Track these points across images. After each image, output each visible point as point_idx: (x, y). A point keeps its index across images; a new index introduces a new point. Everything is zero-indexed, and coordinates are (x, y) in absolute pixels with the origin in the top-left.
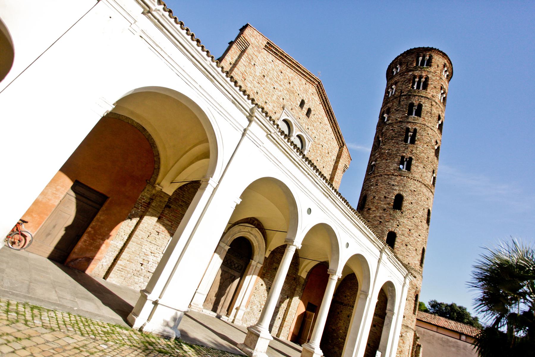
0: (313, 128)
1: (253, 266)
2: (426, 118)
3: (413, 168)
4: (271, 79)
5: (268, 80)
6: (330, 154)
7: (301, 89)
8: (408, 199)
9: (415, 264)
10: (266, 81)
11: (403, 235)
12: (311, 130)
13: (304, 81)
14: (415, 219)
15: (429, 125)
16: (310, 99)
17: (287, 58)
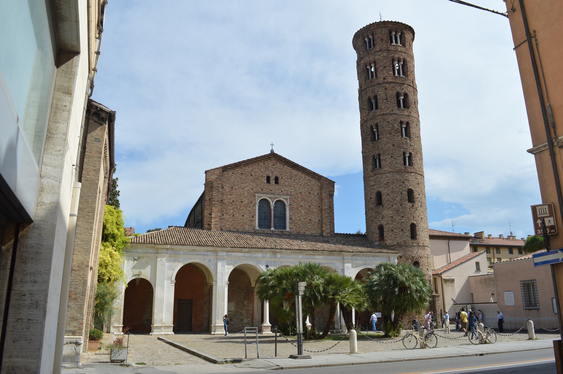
0: (285, 187)
2: (383, 107)
3: (383, 163)
4: (238, 185)
5: (236, 187)
6: (312, 192)
7: (262, 170)
8: (384, 191)
9: (405, 241)
10: (236, 189)
11: (388, 224)
12: (285, 190)
14: (394, 206)
15: (388, 111)
16: (273, 170)
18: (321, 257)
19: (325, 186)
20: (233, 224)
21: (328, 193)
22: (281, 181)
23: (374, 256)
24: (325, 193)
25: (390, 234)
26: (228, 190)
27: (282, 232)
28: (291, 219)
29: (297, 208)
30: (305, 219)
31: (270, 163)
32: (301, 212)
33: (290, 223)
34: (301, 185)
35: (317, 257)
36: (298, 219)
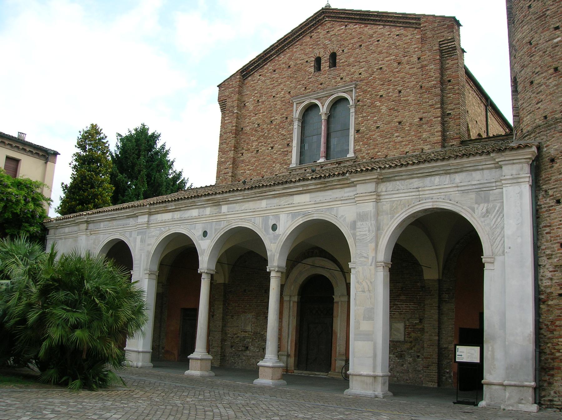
1: (337, 303)
6: (404, 60)
10: (263, 102)
11: (523, 67)
12: (348, 75)
13: (307, 39)
16: (327, 42)
17: (268, 53)
18: (305, 198)
19: (429, 34)
20: (257, 166)
21: (437, 47)
22: (341, 59)
23: (447, 173)
24: (430, 50)
25: (529, 94)
26: (251, 108)
27: (339, 163)
28: (358, 131)
29: (372, 105)
30: (389, 123)
31: (321, 31)
32: (379, 111)
33: (356, 141)
34: (380, 53)
35: (298, 199)
36: (373, 128)
